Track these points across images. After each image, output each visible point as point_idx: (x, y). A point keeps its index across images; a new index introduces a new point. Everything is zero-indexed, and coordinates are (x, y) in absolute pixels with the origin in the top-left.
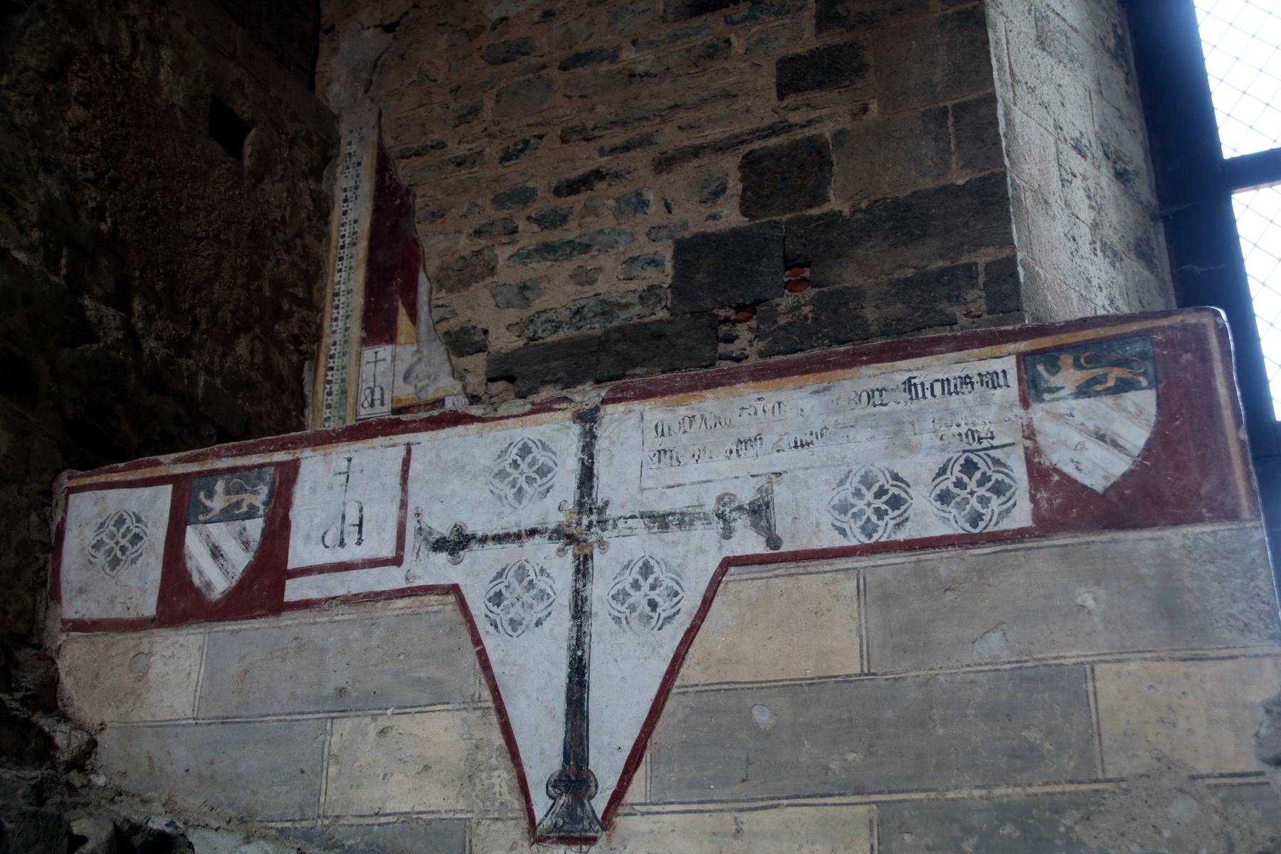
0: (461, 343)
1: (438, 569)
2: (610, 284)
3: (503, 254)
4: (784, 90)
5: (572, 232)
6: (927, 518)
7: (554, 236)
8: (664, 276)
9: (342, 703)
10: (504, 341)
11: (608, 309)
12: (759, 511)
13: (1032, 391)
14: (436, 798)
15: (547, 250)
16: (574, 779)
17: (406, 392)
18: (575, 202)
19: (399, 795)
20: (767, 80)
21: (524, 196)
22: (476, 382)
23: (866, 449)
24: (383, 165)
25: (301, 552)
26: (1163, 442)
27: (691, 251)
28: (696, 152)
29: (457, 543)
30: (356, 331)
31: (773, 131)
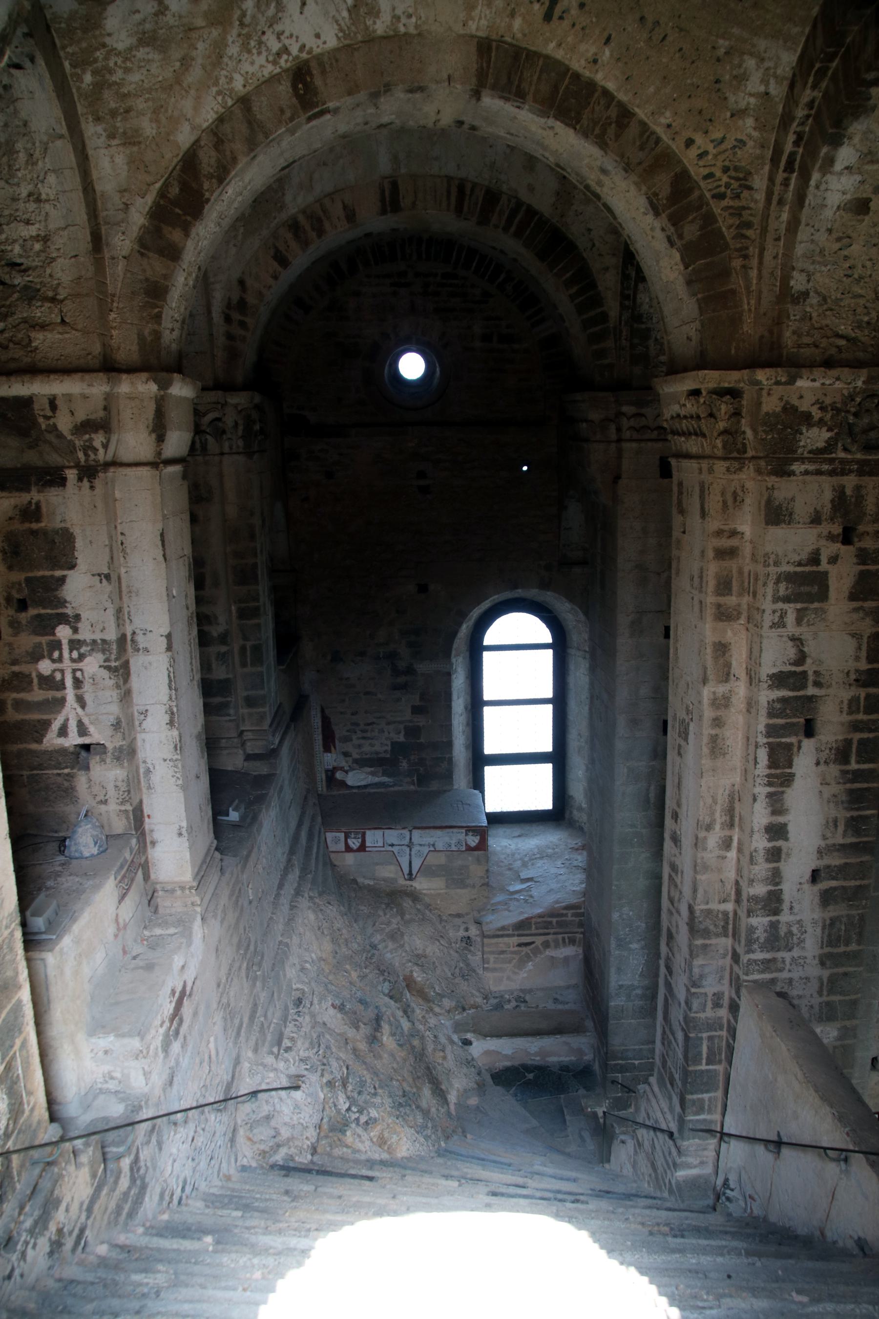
0: (346, 754)
1: (390, 848)
2: (377, 748)
3: (354, 737)
4: (412, 713)
5: (369, 735)
6: (454, 848)
7: (365, 735)
8: (389, 748)
9: (377, 864)
10: (357, 757)
11: (377, 753)
12: (433, 845)
13: (467, 835)
14: (392, 875)
15: (364, 738)
16: (410, 873)
17: (335, 764)
18: (369, 728)
19: (387, 874)
20: (409, 711)
21: (357, 725)
22: (350, 763)
23: (447, 839)
24: (323, 711)
25: (368, 844)
26: (480, 842)
27: (393, 744)
28: (394, 722)
29: (392, 845)
30: (322, 749)
31: (410, 721)
